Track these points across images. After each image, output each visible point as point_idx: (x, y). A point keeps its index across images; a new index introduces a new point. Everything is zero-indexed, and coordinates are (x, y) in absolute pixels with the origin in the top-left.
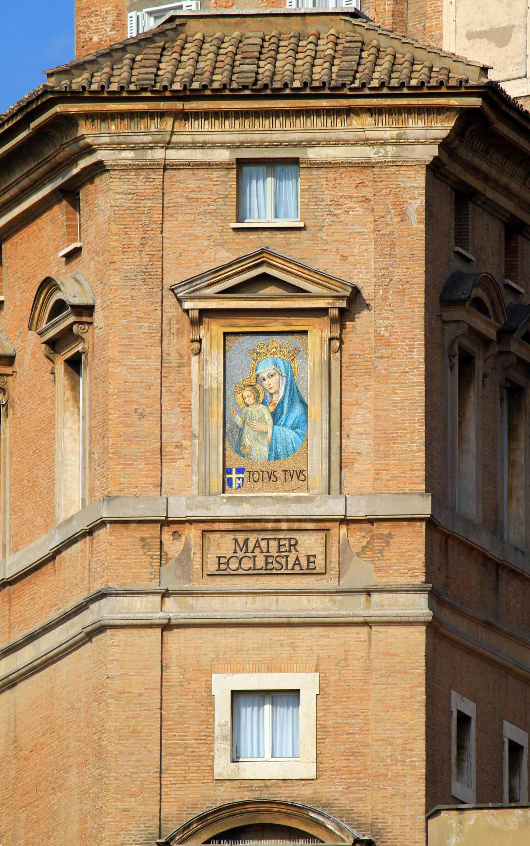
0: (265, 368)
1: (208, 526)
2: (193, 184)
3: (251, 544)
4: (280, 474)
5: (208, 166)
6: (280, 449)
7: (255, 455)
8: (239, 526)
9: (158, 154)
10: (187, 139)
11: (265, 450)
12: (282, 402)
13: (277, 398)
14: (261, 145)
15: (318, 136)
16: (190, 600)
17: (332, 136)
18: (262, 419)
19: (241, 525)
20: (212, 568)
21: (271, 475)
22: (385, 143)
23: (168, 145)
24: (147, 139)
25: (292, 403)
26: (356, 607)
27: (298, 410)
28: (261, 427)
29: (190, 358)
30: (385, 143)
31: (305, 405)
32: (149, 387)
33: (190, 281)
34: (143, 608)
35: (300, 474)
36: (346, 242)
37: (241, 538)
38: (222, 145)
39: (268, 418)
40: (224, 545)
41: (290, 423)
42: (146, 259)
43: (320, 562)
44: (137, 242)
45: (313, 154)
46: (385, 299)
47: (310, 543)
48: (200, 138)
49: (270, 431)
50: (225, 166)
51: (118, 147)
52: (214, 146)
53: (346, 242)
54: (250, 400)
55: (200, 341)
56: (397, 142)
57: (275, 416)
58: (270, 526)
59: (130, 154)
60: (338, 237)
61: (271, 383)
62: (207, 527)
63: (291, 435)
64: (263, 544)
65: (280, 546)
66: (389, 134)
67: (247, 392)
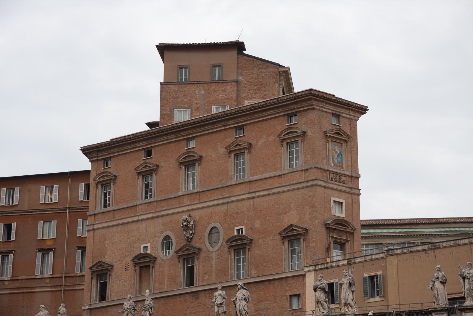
0: (336, 148)
1: (330, 172)
3: (336, 176)
7: (335, 162)
8: (334, 173)
9: (322, 108)
10: (326, 107)
11: (337, 161)
13: (338, 153)
14: (336, 111)
15: (344, 112)
16: (328, 184)
17: (345, 113)
18: (336, 156)
19: (334, 173)
20: (331, 179)
21: (338, 165)
22: (352, 116)
23: (324, 108)
24: (321, 105)
25: (340, 154)
26: (350, 190)
27: (341, 156)
28: (336, 157)
29: (326, 143)
30: (352, 116)
31: (342, 155)
32: (321, 146)
33: (329, 130)
34: (321, 183)
35: (342, 167)
36: (347, 130)
37: (334, 175)
38: (331, 110)
39: (337, 156)
40: (332, 176)
43: (345, 181)
45: (343, 115)
47: (344, 178)
48: (328, 108)
50: (330, 113)
51: (317, 106)
52: (330, 109)
54: (334, 153)
55: (328, 141)
56: (354, 116)
58: (338, 174)
59: (318, 108)
60: (345, 129)
61: (337, 150)
62: (330, 172)
63: (340, 160)
66: (353, 114)
67: (334, 151)
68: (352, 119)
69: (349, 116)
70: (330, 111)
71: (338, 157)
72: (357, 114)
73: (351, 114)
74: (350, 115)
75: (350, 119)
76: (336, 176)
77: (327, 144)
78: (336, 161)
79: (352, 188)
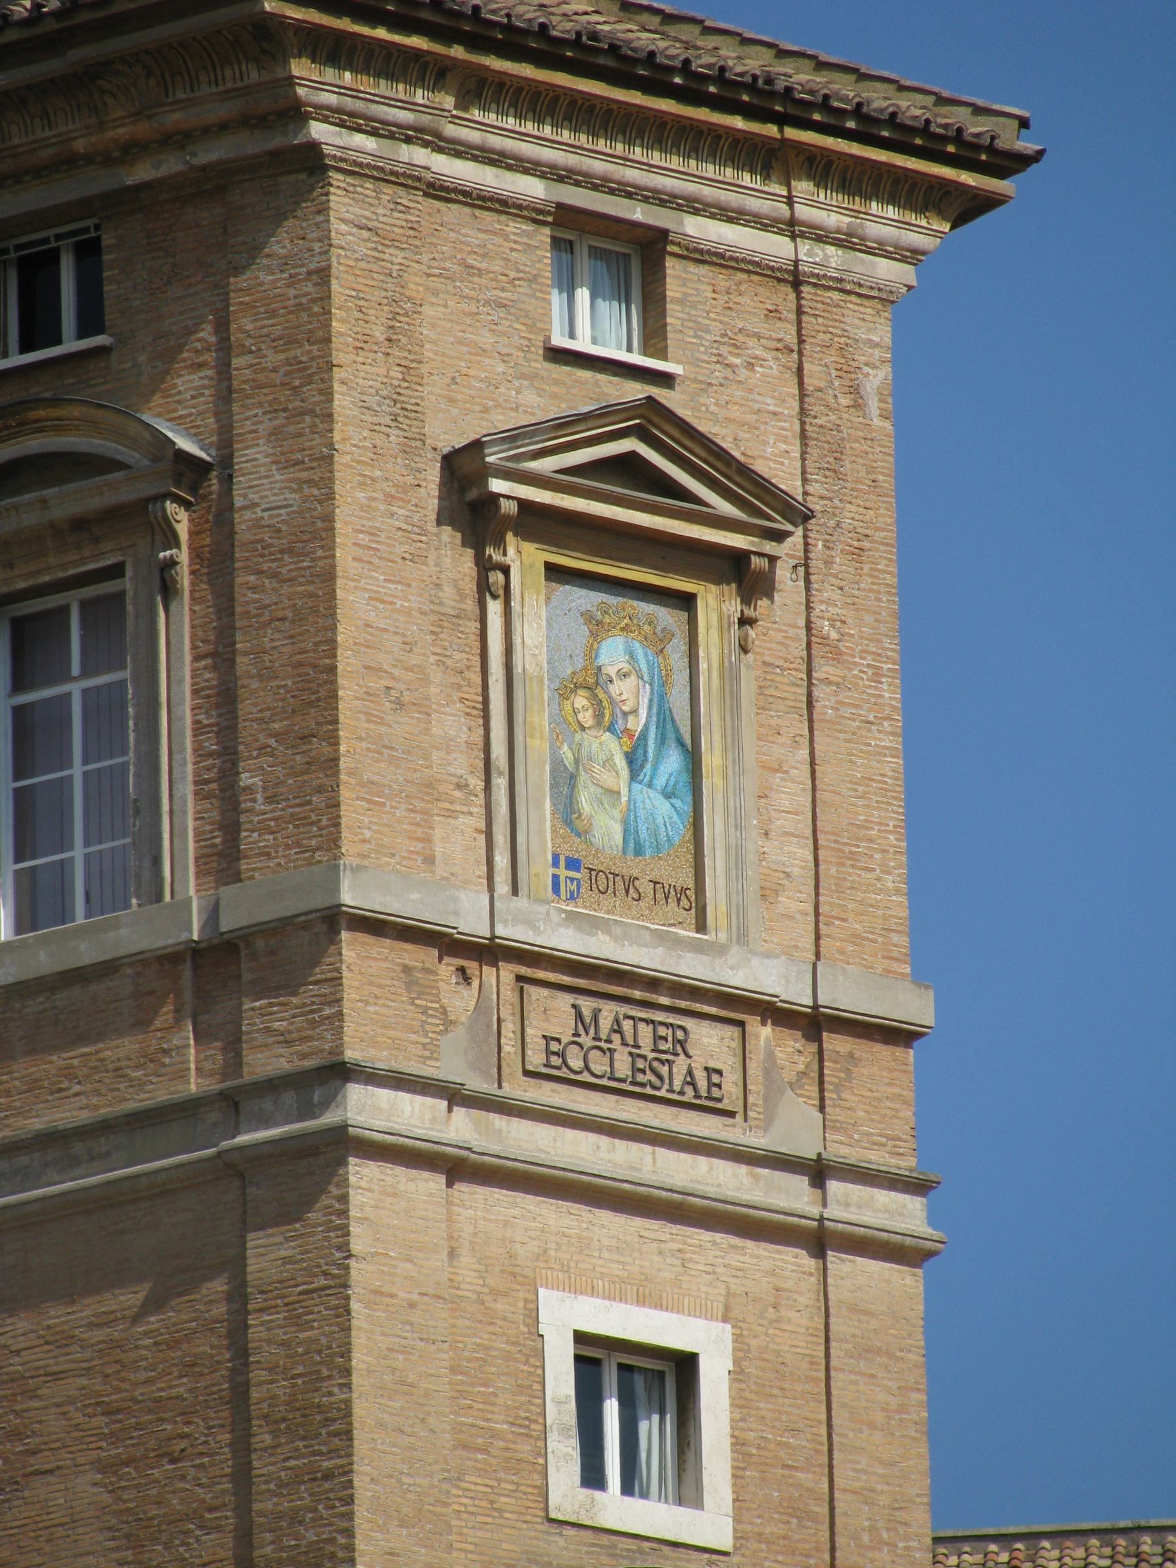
2: (474, 237)
4: (645, 887)
5: (502, 205)
6: (644, 835)
9: (419, 155)
11: (617, 830)
12: (644, 736)
18: (608, 763)
25: (662, 741)
28: (608, 780)
36: (752, 427)
39: (620, 762)
41: (660, 782)
42: (396, 373)
44: (379, 333)
46: (828, 563)
49: (624, 791)
53: (752, 427)
54: (587, 718)
57: (634, 761)
60: (735, 412)
64: (627, 1025)
65: (657, 1038)
68: (821, 283)
69: (776, 247)
70: (533, 188)
71: (634, 776)
72: (891, 212)
73: (803, 212)
74: (792, 228)
75: (795, 278)
76: (606, 1023)
77: (494, 608)
78: (607, 830)
79: (818, 1172)
